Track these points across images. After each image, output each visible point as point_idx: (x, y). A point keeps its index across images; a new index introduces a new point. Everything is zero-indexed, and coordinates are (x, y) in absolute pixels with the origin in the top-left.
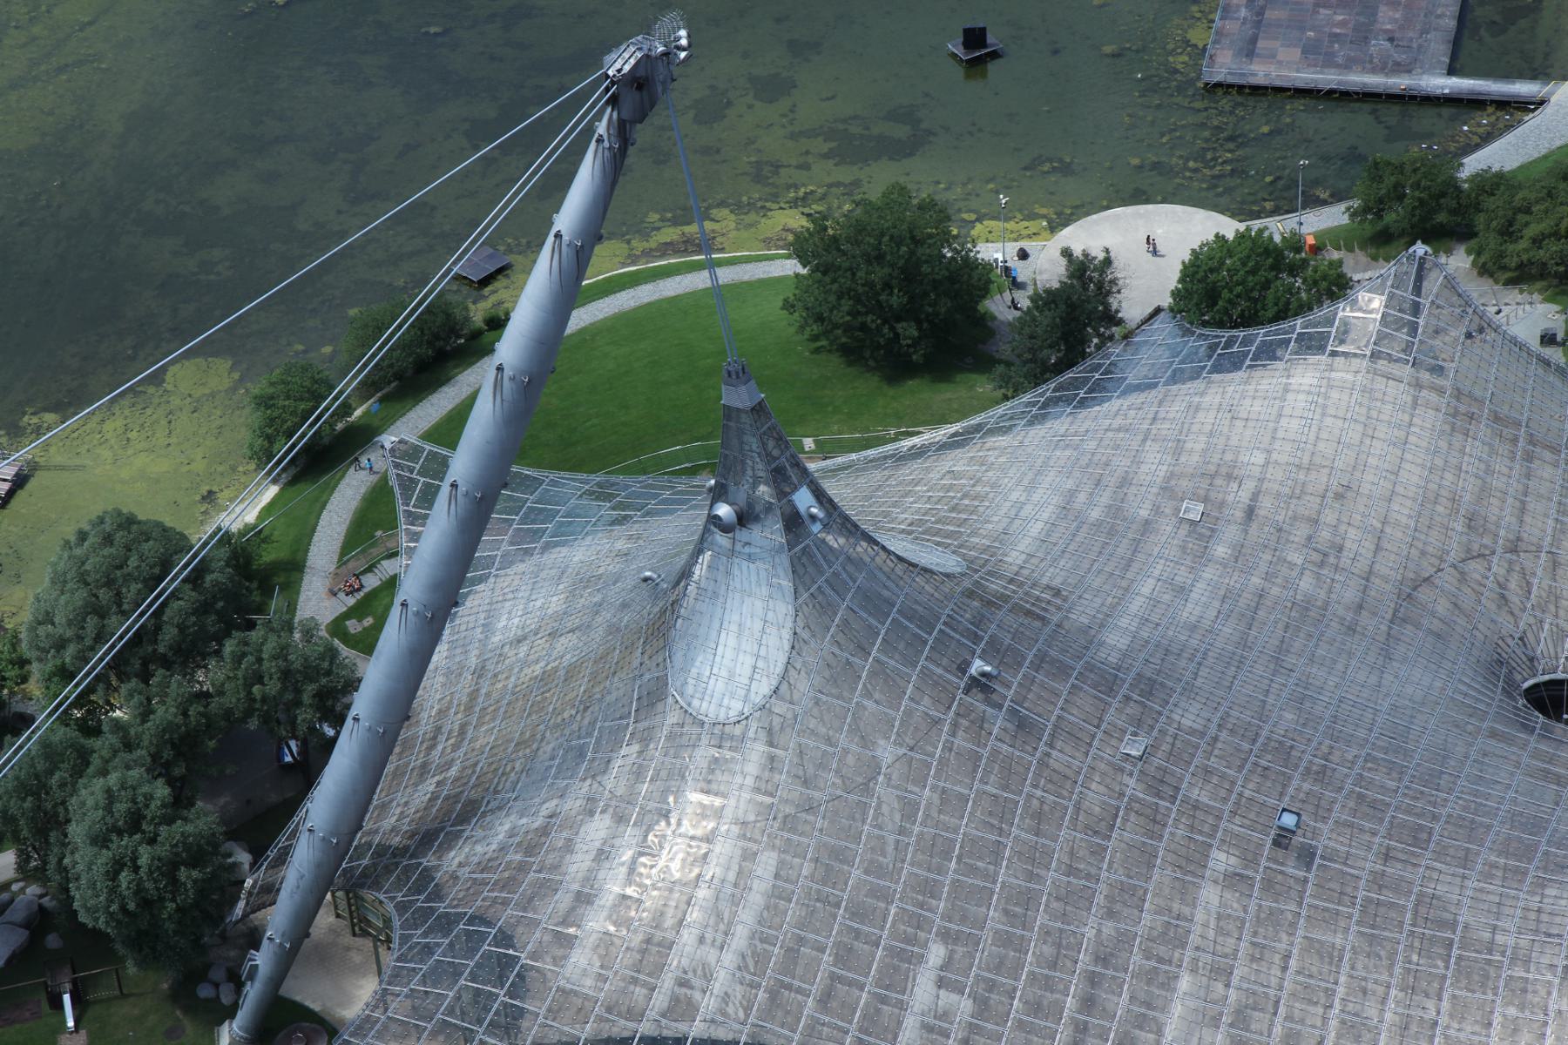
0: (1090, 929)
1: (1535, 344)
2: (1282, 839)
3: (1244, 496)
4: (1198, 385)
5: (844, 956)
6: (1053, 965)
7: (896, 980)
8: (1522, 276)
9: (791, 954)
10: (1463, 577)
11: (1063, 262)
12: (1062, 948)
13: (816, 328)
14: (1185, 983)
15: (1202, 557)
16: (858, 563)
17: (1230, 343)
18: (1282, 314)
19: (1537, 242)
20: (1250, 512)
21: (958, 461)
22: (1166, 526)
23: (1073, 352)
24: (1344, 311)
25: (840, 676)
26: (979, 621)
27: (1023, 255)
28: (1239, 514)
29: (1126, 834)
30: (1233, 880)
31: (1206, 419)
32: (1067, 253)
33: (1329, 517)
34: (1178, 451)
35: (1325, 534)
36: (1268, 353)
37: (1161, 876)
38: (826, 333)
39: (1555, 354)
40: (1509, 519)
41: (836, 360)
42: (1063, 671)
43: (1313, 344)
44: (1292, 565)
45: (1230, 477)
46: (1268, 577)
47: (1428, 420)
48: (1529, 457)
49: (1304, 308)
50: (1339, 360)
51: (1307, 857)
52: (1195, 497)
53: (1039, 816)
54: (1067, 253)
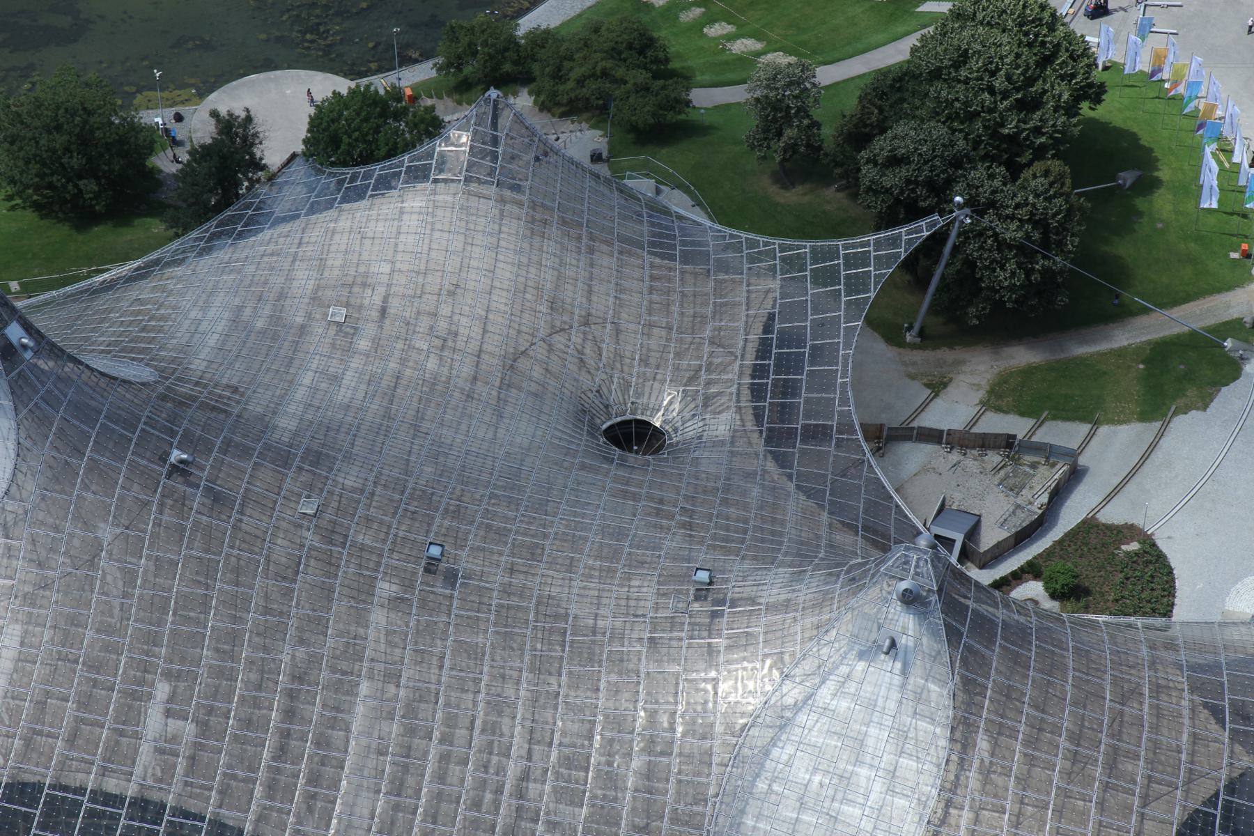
0: (287, 655)
1: (586, 161)
2: (431, 566)
3: (378, 300)
4: (332, 213)
5: (85, 703)
6: (259, 688)
7: (130, 716)
8: (572, 109)
9: (41, 705)
10: (551, 348)
11: (213, 121)
12: (265, 673)
13: (10, 190)
14: (364, 688)
15: (349, 350)
16: (67, 381)
17: (354, 178)
18: (392, 153)
19: (581, 82)
20: (383, 311)
21: (143, 291)
22: (318, 329)
23: (229, 197)
24: (441, 147)
25: (61, 475)
26: (173, 419)
27: (179, 118)
28: (375, 314)
29: (311, 574)
30: (397, 603)
31: (341, 241)
32: (214, 114)
33: (445, 310)
34: (322, 266)
35: (443, 325)
36: (385, 184)
37: (339, 606)
38: (19, 194)
39: (603, 170)
40: (580, 299)
41: (30, 216)
42: (246, 452)
43: (419, 174)
44: (420, 350)
45: (364, 285)
46: (403, 362)
47: (513, 228)
48: (591, 251)
49: (409, 147)
50: (441, 186)
51: (451, 578)
52: (338, 303)
53: (237, 571)
54: (214, 114)
